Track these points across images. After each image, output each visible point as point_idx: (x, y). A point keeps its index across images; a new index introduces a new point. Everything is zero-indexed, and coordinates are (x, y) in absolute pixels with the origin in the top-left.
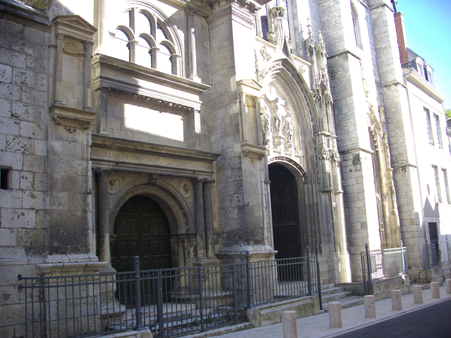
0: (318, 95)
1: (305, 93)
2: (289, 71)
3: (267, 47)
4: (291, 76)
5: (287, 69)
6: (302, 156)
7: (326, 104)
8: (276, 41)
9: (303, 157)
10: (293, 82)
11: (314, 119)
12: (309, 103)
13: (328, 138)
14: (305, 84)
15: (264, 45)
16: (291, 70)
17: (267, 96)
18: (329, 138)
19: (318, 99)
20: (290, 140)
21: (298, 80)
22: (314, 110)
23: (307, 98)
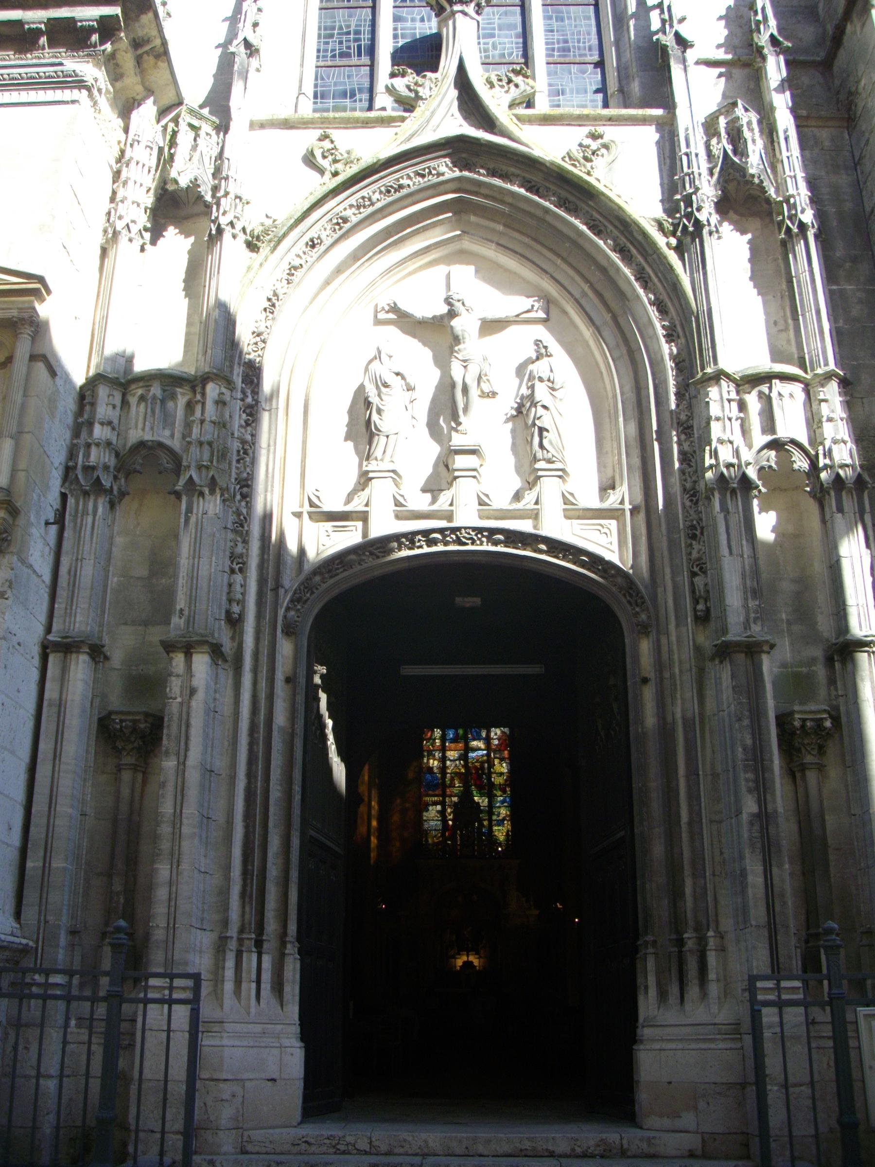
0: (689, 216)
1: (616, 233)
2: (504, 177)
3: (335, 134)
4: (522, 191)
5: (493, 173)
6: (627, 506)
7: (784, 243)
8: (417, 92)
9: (632, 511)
10: (547, 211)
11: (679, 329)
12: (649, 270)
13: (765, 388)
14: (602, 198)
15: (318, 133)
16: (512, 170)
17: (403, 306)
18: (770, 388)
19: (692, 233)
20: (539, 455)
21: (564, 194)
22: (675, 286)
23: (634, 251)
